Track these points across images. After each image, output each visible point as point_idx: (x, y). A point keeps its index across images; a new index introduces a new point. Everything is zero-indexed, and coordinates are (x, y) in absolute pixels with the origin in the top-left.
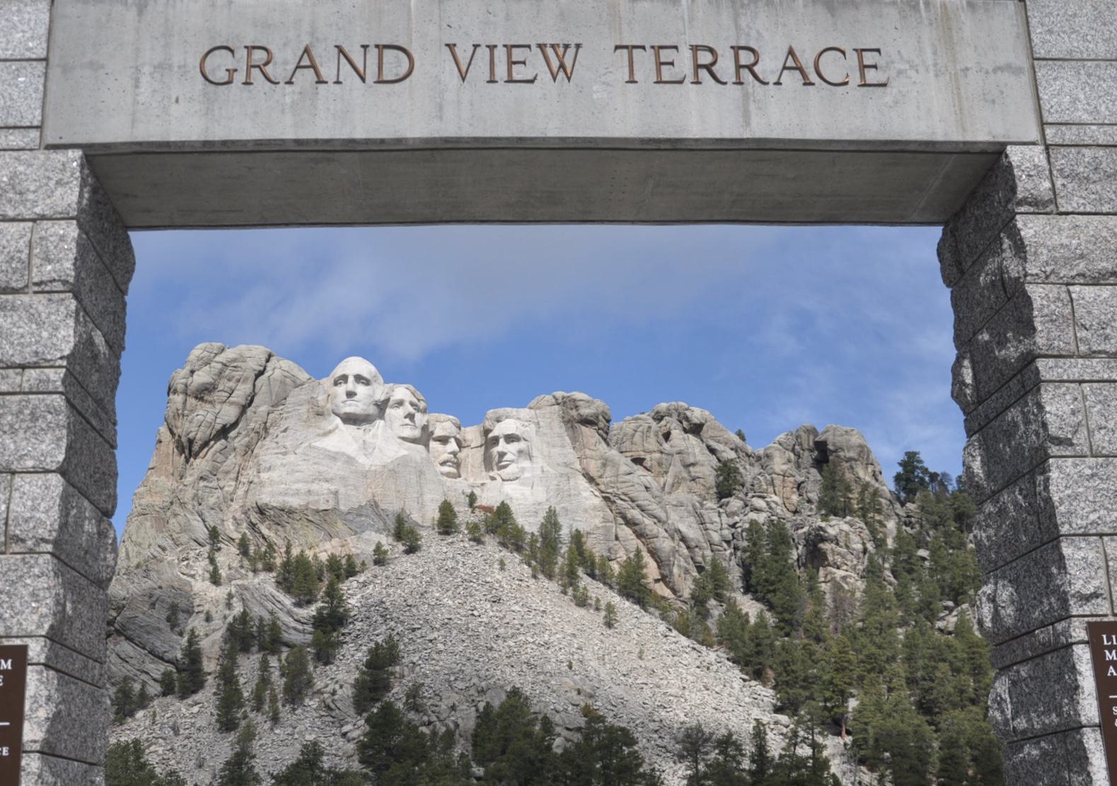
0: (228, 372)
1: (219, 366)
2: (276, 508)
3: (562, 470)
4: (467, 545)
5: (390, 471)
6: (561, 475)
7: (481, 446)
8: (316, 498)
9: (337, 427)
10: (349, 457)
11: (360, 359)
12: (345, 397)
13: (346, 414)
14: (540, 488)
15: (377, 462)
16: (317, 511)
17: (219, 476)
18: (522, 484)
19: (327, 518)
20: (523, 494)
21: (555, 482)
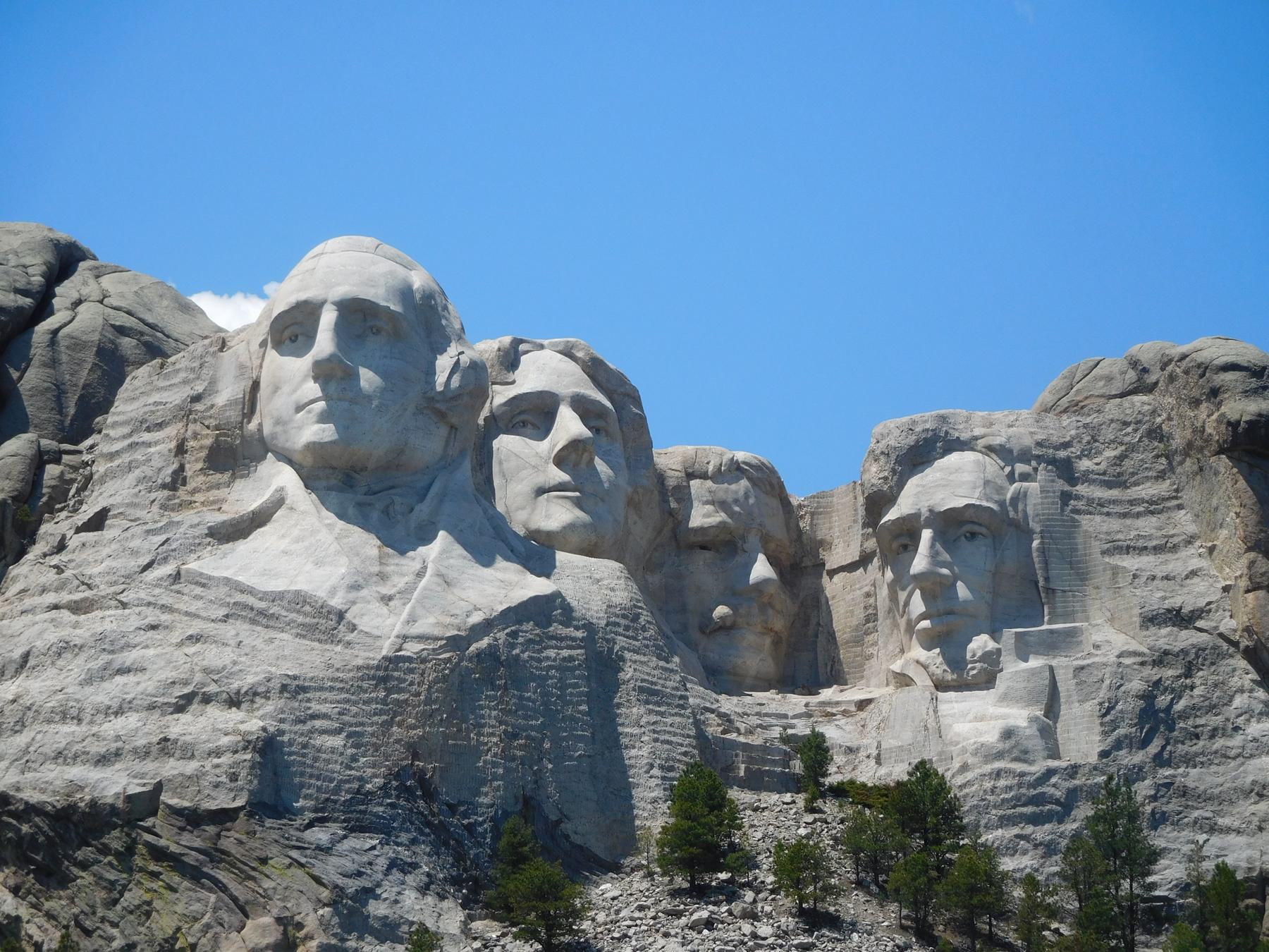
3: (1166, 637)
4: (765, 930)
5: (479, 654)
6: (1162, 658)
7: (863, 561)
8: (191, 767)
9: (278, 502)
10: (323, 611)
11: (369, 241)
12: (312, 389)
13: (313, 447)
15: (426, 625)
16: (193, 819)
18: (1004, 698)
19: (228, 843)
20: (1008, 734)
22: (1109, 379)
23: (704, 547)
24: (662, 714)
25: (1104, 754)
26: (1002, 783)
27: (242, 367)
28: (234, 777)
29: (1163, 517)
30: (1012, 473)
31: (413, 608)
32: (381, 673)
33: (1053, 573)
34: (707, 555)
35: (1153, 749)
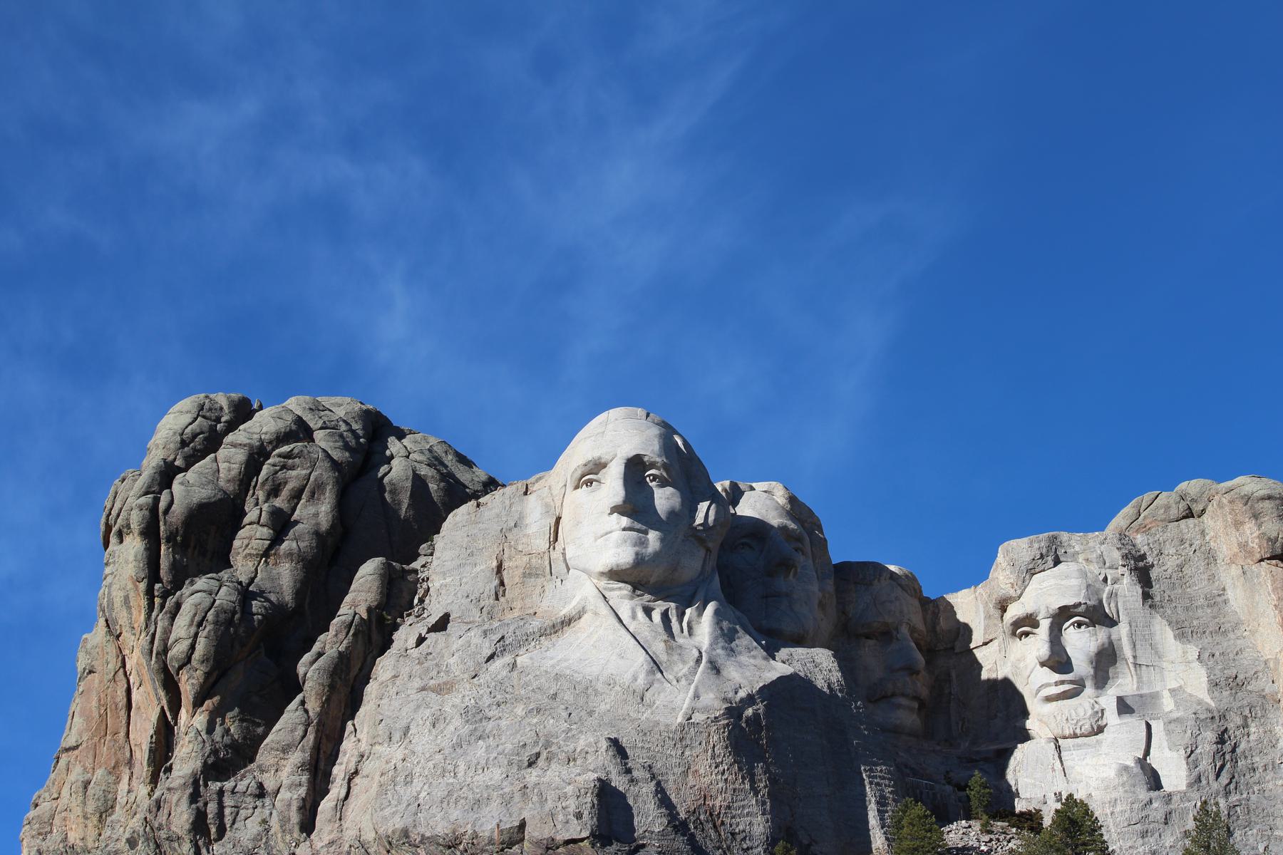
0: (265, 470)
1: (240, 456)
2: (433, 840)
11: (641, 412)
14: (1168, 753)
16: (550, 846)
17: (265, 756)
21: (1210, 735)
22: (1167, 507)
23: (868, 637)
24: (876, 765)
25: (1190, 785)
26: (1119, 808)
27: (547, 505)
28: (579, 816)
29: (1216, 609)
30: (1105, 580)
31: (697, 688)
32: (678, 736)
33: (1139, 653)
34: (871, 642)
35: (1224, 779)
